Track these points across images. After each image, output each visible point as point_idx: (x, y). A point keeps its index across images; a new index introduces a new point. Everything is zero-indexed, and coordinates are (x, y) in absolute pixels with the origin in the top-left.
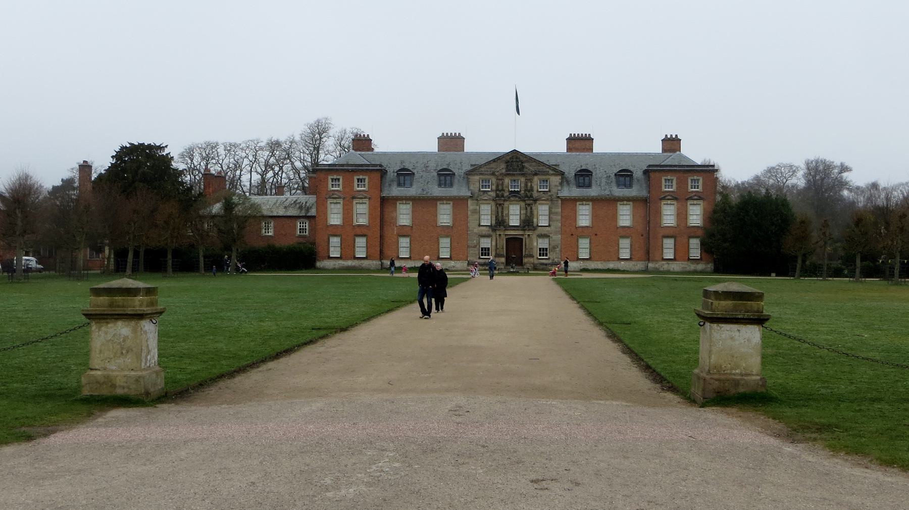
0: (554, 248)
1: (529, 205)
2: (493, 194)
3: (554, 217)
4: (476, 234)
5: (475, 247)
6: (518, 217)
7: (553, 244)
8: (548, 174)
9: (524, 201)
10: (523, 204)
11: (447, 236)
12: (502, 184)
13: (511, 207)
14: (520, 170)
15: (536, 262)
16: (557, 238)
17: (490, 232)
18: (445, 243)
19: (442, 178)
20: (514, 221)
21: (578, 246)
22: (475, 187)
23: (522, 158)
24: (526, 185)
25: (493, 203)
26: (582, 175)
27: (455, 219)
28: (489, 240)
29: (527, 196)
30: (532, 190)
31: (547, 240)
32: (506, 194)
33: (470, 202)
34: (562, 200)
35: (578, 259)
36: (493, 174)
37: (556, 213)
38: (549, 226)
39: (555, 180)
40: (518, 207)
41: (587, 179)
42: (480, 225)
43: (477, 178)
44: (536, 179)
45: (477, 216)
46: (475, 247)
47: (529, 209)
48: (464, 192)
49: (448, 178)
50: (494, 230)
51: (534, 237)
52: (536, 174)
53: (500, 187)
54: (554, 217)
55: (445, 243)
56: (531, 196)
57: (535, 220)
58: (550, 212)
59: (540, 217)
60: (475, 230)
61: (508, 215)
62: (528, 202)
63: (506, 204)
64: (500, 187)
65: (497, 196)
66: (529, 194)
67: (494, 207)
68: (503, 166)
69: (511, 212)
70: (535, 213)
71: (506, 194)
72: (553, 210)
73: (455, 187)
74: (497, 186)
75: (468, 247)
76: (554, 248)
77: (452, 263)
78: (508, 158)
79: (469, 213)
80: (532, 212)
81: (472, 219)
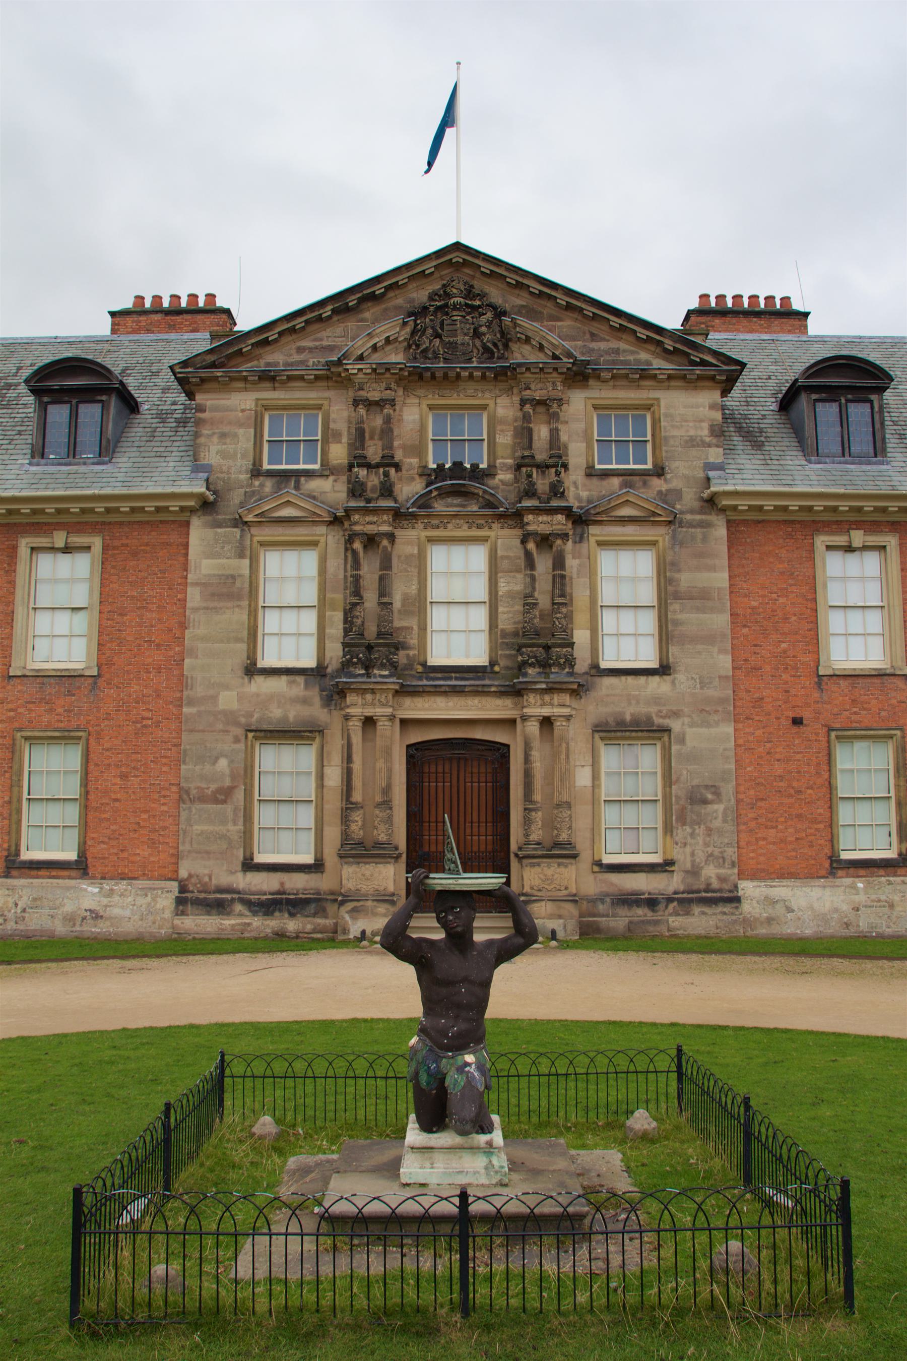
0: (697, 798)
1: (545, 541)
2: (332, 491)
3: (688, 618)
4: (230, 718)
5: (223, 795)
6: (479, 618)
7: (688, 775)
8: (645, 375)
9: (516, 517)
10: (507, 538)
11: (65, 738)
12: (387, 433)
13: (441, 559)
14: (488, 353)
15: (593, 886)
16: (711, 742)
17: (317, 711)
18: (53, 770)
19: (59, 414)
20: (458, 634)
21: (831, 787)
22: (229, 452)
23: (496, 294)
24: (525, 434)
25: (333, 539)
26: (831, 393)
27: (106, 639)
28: (305, 757)
29: (530, 493)
30: (557, 461)
31: (648, 757)
32: (409, 489)
33: (199, 534)
34: (729, 523)
35: (837, 867)
36: (333, 375)
37: (702, 597)
38: (664, 670)
39: (688, 411)
40: (476, 558)
41: (858, 412)
42: (252, 670)
43: (243, 401)
44: (578, 403)
45: (238, 616)
46: (223, 795)
47: (544, 564)
48: (166, 476)
49: (90, 413)
50: (335, 695)
51: (576, 734)
52: (580, 374)
53: (374, 451)
54: (688, 618)
55: (53, 770)
56: (557, 490)
57: (581, 636)
58: (668, 593)
59: (608, 621)
60: (228, 700)
61: (419, 605)
62: (538, 524)
63: (409, 538)
64: (374, 451)
65: (356, 490)
66: (542, 484)
67: (336, 565)
68: (390, 327)
69: (437, 589)
70: (580, 593)
71: (409, 489)
72: (686, 579)
73: (124, 461)
74: (359, 436)
75: (183, 796)
76: (697, 798)
77: (88, 894)
78: (420, 295)
79: (194, 597)
80: (560, 581)
81: (209, 632)
